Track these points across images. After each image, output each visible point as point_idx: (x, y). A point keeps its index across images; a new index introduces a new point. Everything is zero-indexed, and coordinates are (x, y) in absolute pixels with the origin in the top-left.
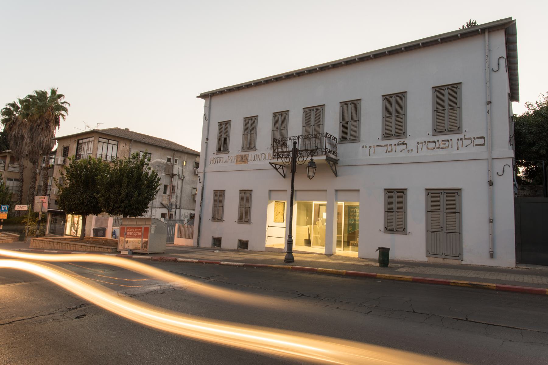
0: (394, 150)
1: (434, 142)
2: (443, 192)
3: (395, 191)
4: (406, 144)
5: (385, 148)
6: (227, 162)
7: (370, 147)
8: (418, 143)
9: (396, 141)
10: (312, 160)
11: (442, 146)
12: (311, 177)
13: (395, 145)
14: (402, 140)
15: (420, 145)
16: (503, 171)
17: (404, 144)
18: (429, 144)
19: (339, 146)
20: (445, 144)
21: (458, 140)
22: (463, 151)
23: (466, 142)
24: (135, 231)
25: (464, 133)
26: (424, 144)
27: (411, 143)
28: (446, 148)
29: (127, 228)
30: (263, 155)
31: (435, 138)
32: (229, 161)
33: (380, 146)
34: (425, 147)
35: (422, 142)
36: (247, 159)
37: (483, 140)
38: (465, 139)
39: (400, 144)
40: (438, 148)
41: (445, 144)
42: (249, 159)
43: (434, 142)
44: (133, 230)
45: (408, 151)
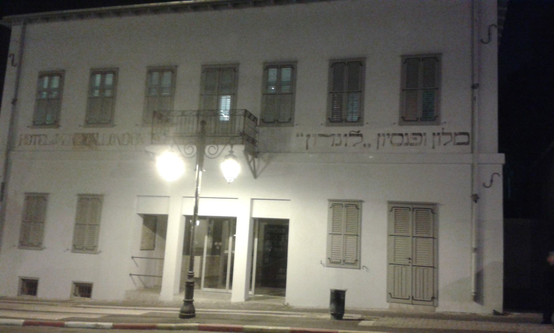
1: (401, 135)
4: (361, 135)
5: (330, 140)
7: (308, 136)
8: (379, 135)
11: (412, 141)
13: (346, 135)
14: (356, 129)
15: (382, 138)
17: (358, 135)
18: (395, 137)
19: (261, 130)
21: (434, 134)
26: (386, 137)
27: (369, 133)
28: (416, 144)
35: (384, 135)
38: (444, 134)
39: (353, 135)
40: (407, 144)
41: (416, 139)
42: (100, 140)
43: (401, 135)
45: (365, 145)
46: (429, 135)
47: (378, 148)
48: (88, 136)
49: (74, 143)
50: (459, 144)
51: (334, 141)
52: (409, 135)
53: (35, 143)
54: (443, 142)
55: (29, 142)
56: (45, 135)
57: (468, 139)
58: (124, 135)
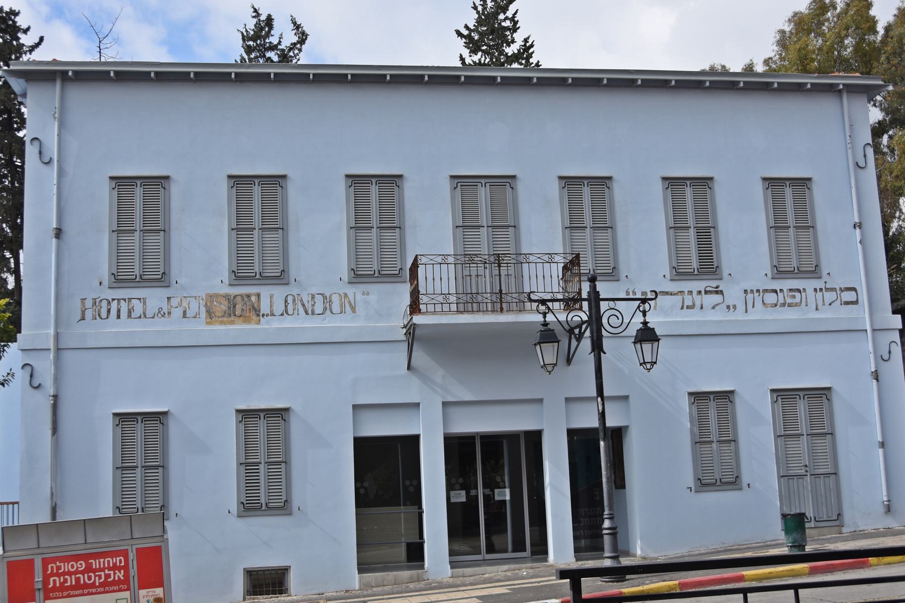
0: (698, 304)
1: (775, 291)
2: (801, 394)
3: (712, 397)
4: (721, 292)
6: (161, 314)
8: (746, 291)
9: (701, 285)
10: (645, 323)
11: (789, 301)
12: (550, 368)
13: (700, 292)
14: (714, 284)
15: (750, 296)
16: (890, 352)
17: (717, 292)
20: (794, 297)
22: (826, 314)
24: (89, 569)
26: (756, 294)
28: (796, 305)
29: (45, 562)
30: (319, 299)
31: (776, 285)
32: (177, 313)
36: (257, 311)
37: (854, 293)
38: (827, 290)
40: (784, 305)
41: (794, 297)
42: (265, 308)
43: (775, 291)
44: (82, 565)
45: (728, 307)
46: (810, 292)
47: (746, 311)
48: (239, 298)
49: (210, 313)
50: (847, 303)
51: (683, 302)
52: (785, 291)
53: (119, 317)
54: (827, 302)
55: (104, 315)
56: (143, 300)
58: (313, 297)
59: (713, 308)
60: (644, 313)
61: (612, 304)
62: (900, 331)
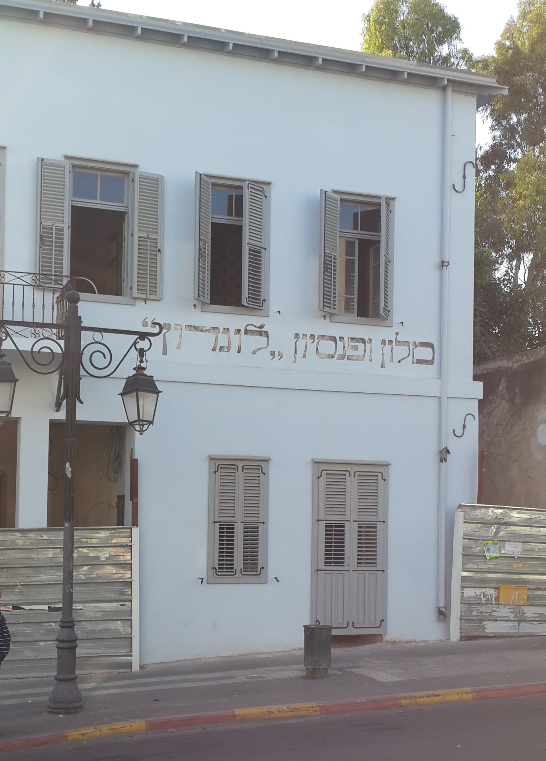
0: (234, 348)
1: (334, 339)
4: (266, 334)
8: (297, 335)
10: (140, 369)
11: (350, 352)
13: (239, 331)
15: (301, 343)
16: (464, 427)
17: (260, 333)
18: (323, 342)
20: (356, 348)
21: (384, 341)
23: (401, 351)
25: (397, 328)
33: (196, 328)
34: (312, 348)
37: (430, 350)
38: (399, 343)
39: (253, 332)
40: (342, 357)
41: (356, 348)
43: (334, 339)
45: (273, 354)
46: (377, 344)
50: (420, 362)
51: (216, 342)
54: (396, 359)
57: (430, 353)
59: (254, 353)
60: (142, 353)
61: (98, 336)
62: (480, 401)
